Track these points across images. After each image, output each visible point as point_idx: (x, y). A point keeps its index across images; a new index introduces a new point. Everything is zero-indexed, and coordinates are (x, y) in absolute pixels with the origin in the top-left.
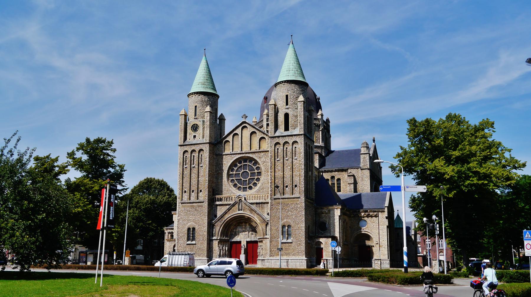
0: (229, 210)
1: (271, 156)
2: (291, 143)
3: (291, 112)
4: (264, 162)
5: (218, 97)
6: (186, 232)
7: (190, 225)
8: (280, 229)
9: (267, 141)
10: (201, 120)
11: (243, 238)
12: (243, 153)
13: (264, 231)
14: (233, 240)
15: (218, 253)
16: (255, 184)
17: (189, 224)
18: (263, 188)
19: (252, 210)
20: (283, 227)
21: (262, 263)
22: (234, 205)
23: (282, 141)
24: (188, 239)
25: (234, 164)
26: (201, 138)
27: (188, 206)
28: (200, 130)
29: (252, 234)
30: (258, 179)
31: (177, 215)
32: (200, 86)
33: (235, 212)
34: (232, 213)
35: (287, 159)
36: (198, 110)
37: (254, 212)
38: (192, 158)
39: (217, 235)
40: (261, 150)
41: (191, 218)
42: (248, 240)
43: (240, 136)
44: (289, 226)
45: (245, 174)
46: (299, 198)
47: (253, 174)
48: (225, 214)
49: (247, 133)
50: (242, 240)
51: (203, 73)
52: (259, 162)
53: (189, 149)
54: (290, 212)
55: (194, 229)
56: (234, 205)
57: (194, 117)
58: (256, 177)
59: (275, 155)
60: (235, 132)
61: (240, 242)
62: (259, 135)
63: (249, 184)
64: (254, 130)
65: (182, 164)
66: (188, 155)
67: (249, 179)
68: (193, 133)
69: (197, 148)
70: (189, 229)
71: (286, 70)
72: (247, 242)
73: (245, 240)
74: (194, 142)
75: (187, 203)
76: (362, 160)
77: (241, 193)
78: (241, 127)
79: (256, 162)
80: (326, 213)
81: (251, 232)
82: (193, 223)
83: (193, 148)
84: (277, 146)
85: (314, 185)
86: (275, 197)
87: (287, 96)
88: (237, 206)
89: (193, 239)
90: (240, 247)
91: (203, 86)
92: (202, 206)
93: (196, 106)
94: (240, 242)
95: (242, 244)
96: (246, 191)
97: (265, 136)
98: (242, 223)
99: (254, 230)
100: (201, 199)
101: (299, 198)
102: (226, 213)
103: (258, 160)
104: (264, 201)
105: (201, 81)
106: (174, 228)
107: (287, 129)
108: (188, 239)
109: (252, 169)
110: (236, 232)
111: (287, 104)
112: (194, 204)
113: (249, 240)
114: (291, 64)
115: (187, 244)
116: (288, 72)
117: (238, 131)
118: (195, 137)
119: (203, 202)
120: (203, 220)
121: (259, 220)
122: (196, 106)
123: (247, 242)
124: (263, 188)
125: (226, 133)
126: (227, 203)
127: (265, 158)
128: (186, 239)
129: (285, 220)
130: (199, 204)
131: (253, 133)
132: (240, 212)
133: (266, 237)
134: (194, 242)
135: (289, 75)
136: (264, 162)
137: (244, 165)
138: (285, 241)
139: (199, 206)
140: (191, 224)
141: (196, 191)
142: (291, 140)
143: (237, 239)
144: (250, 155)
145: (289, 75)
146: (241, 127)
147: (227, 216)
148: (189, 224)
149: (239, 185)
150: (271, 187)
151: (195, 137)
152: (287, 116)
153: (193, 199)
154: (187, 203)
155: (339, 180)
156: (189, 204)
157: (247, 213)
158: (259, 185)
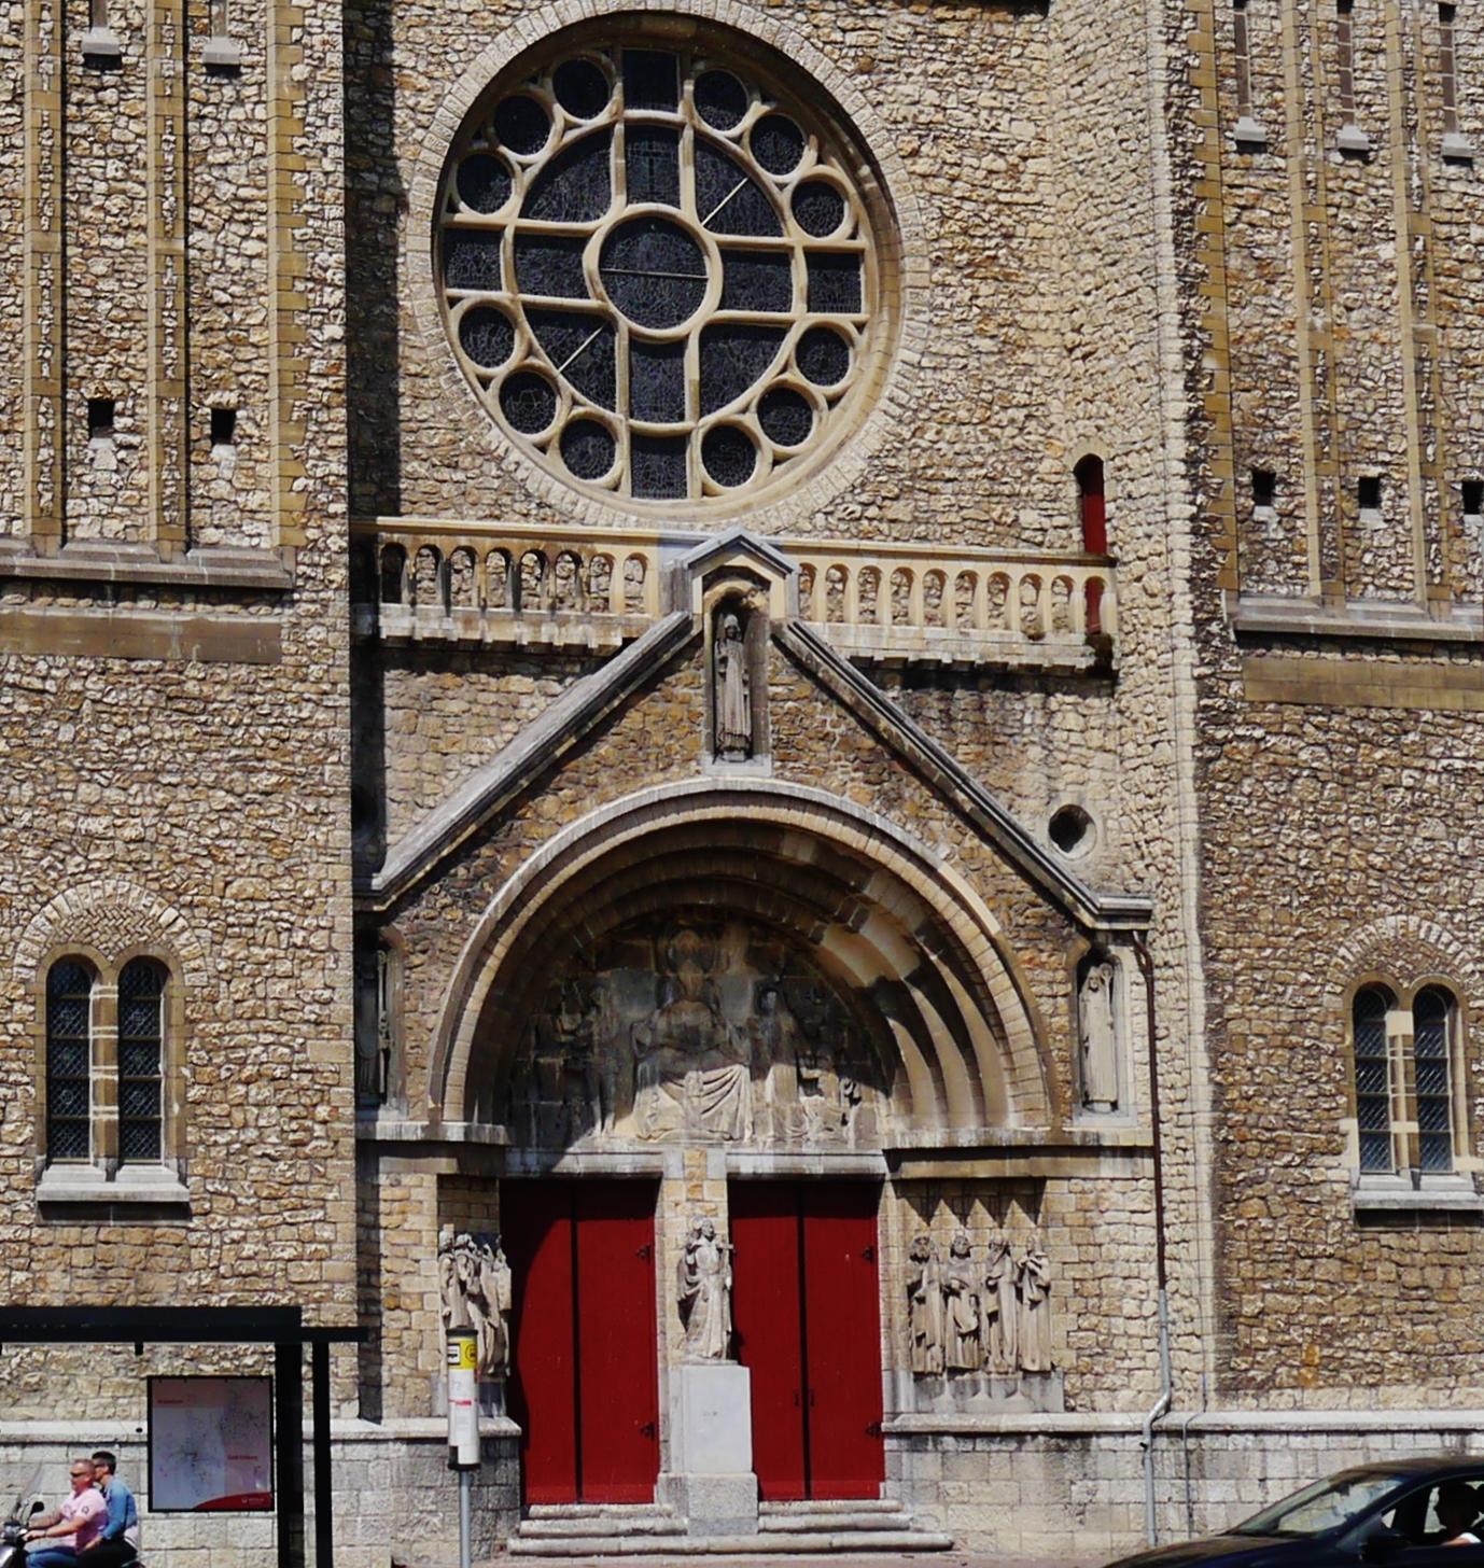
0: (588, 728)
6: (28, 1016)
7: (112, 912)
8: (1339, 1035)
11: (695, 1136)
14: (574, 1162)
17: (70, 901)
18: (921, 481)
19: (895, 760)
20: (1370, 1003)
21: (1059, 1482)
22: (650, 674)
24: (63, 1135)
25: (506, 111)
27: (48, 630)
29: (810, 1086)
30: (826, 353)
33: (678, 774)
34: (629, 774)
37: (914, 791)
39: (419, 1084)
41: (97, 806)
42: (747, 1166)
44: (1433, 1004)
45: (654, 259)
48: (538, 788)
50: (672, 1164)
52: (862, 118)
54: (1436, 828)
55: (145, 977)
56: (650, 674)
61: (636, 1195)
63: (712, 396)
67: (711, 332)
70: (68, 978)
72: (746, 1194)
73: (718, 1164)
75: (36, 585)
77: (709, 514)
79: (803, 111)
81: (780, 1072)
82: (138, 897)
88: (686, 686)
89: (137, 1137)
92: (260, 651)
94: (636, 1195)
96: (672, 486)
98: (661, 924)
99: (853, 1038)
100: (248, 540)
102: (541, 774)
103: (846, 92)
104: (1029, 655)
108: (63, 1135)
110: (580, 1047)
112: (143, 611)
113: (758, 1161)
115: (53, 1210)
119: (277, 595)
120: (283, 854)
123: (746, 1194)
124: (921, 481)
126: (521, 633)
127: (936, 80)
128: (22, 1127)
129: (1389, 925)
130: (224, 615)
133: (1083, 1125)
137: (635, 130)
138: (1390, 1189)
139: (217, 649)
140: (94, 904)
141: (148, 415)
143: (610, 1145)
147: (565, 828)
148: (70, 901)
150: (1197, 484)
153: (103, 534)
154: (36, 585)
156: (62, 609)
157: (830, 793)
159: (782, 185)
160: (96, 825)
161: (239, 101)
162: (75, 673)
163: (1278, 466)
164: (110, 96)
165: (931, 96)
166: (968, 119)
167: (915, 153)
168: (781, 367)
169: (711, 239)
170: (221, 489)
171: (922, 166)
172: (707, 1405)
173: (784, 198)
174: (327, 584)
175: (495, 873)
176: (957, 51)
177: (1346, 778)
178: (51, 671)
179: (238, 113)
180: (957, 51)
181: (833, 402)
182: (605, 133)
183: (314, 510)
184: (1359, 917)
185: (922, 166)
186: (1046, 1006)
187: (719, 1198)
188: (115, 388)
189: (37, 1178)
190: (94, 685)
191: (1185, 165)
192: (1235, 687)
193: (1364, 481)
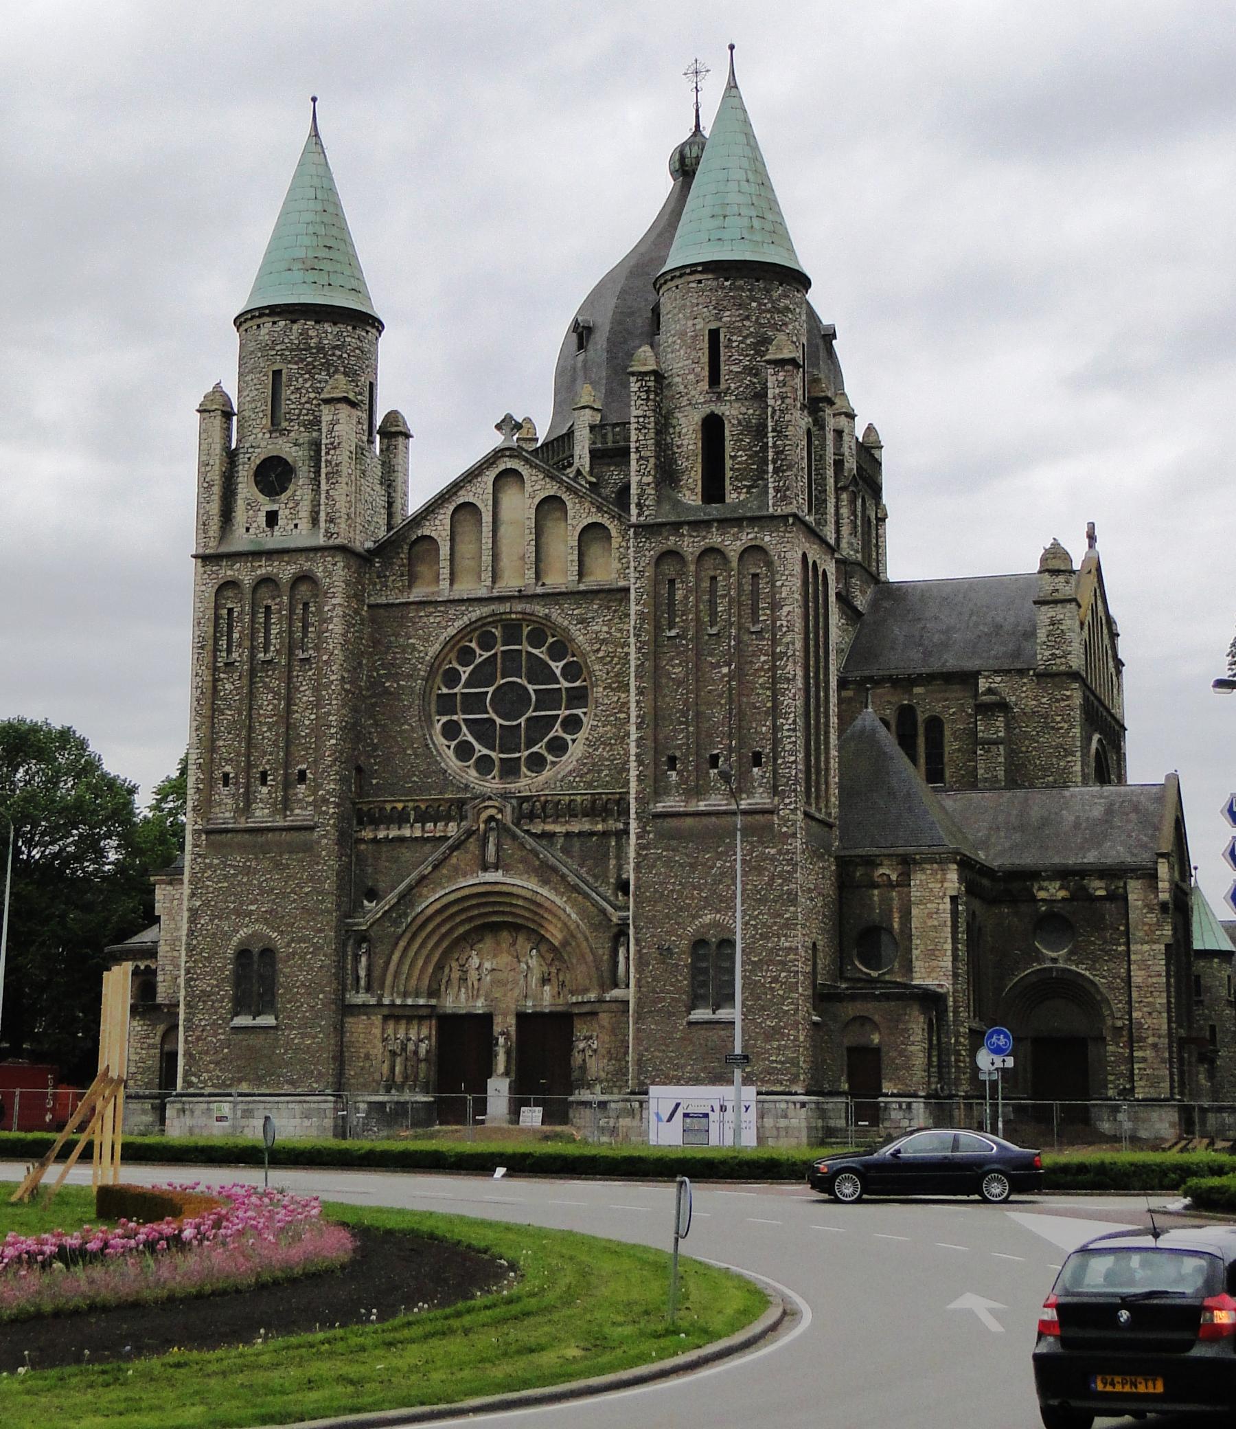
1: (641, 615)
2: (734, 557)
3: (731, 411)
4: (610, 643)
5: (376, 324)
9: (616, 541)
10: (305, 437)
12: (501, 599)
13: (605, 967)
15: (385, 1068)
16: (558, 747)
23: (690, 545)
24: (240, 1006)
26: (304, 525)
28: (300, 489)
30: (573, 724)
31: (186, 889)
32: (298, 275)
34: (450, 879)
35: (714, 631)
36: (286, 392)
38: (261, 618)
40: (589, 583)
43: (487, 518)
46: (771, 812)
47: (549, 699)
49: (519, 507)
51: (309, 217)
53: (246, 575)
57: (267, 421)
58: (563, 713)
59: (663, 609)
60: (464, 497)
61: (486, 1020)
62: (580, 514)
63: (531, 743)
64: (552, 489)
65: (209, 648)
66: (240, 607)
68: (262, 498)
69: (286, 571)
70: (243, 954)
71: (708, 211)
72: (521, 1017)
74: (275, 540)
76: (1042, 635)
78: (490, 476)
80: (891, 885)
83: (265, 568)
84: (669, 569)
85: (834, 753)
86: (660, 807)
87: (714, 335)
90: (489, 1043)
91: (312, 275)
92: (308, 848)
93: (277, 374)
94: (486, 1020)
95: (497, 1029)
97: (605, 520)
101: (771, 812)
105: (301, 253)
106: (163, 949)
107: (713, 490)
109: (540, 672)
111: (714, 379)
114: (733, 186)
115: (237, 1029)
116: (718, 222)
117: (480, 493)
118: (272, 518)
121: (582, 912)
122: (277, 374)
123: (521, 1017)
125: (415, 502)
129: (707, 919)
131: (549, 507)
132: (491, 876)
134: (268, 1020)
135: (726, 235)
136: (604, 641)
142: (733, 543)
144: (540, 610)
145: (726, 235)
146: (490, 476)
149: (480, 750)
150: (640, 762)
151: (272, 518)
152: (712, 427)
153: (261, 815)
155: (935, 725)
158: (577, 750)
159: (557, 667)
160: (253, 907)
161: (311, 669)
162: (248, 860)
163: (678, 754)
164: (270, 673)
165: (605, 629)
166: (619, 635)
167: (599, 650)
168: (557, 731)
169: (530, 688)
170: (301, 796)
171: (601, 654)
172: (498, 1089)
173: (558, 672)
174: (328, 825)
175: (406, 915)
176: (615, 611)
177: (693, 866)
178: (238, 859)
179: (310, 673)
180: (615, 611)
181: (574, 741)
182: (496, 654)
183: (325, 801)
184: (695, 917)
185: (601, 654)
186: (600, 952)
187: (512, 1020)
188: (268, 767)
189: (232, 1019)
190: (254, 864)
191: (640, 648)
192: (651, 836)
193: (712, 756)
